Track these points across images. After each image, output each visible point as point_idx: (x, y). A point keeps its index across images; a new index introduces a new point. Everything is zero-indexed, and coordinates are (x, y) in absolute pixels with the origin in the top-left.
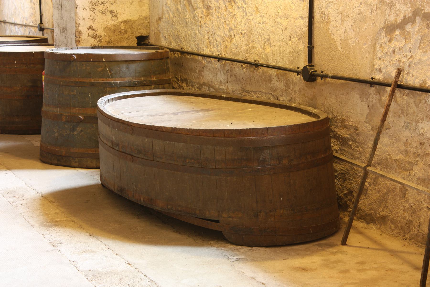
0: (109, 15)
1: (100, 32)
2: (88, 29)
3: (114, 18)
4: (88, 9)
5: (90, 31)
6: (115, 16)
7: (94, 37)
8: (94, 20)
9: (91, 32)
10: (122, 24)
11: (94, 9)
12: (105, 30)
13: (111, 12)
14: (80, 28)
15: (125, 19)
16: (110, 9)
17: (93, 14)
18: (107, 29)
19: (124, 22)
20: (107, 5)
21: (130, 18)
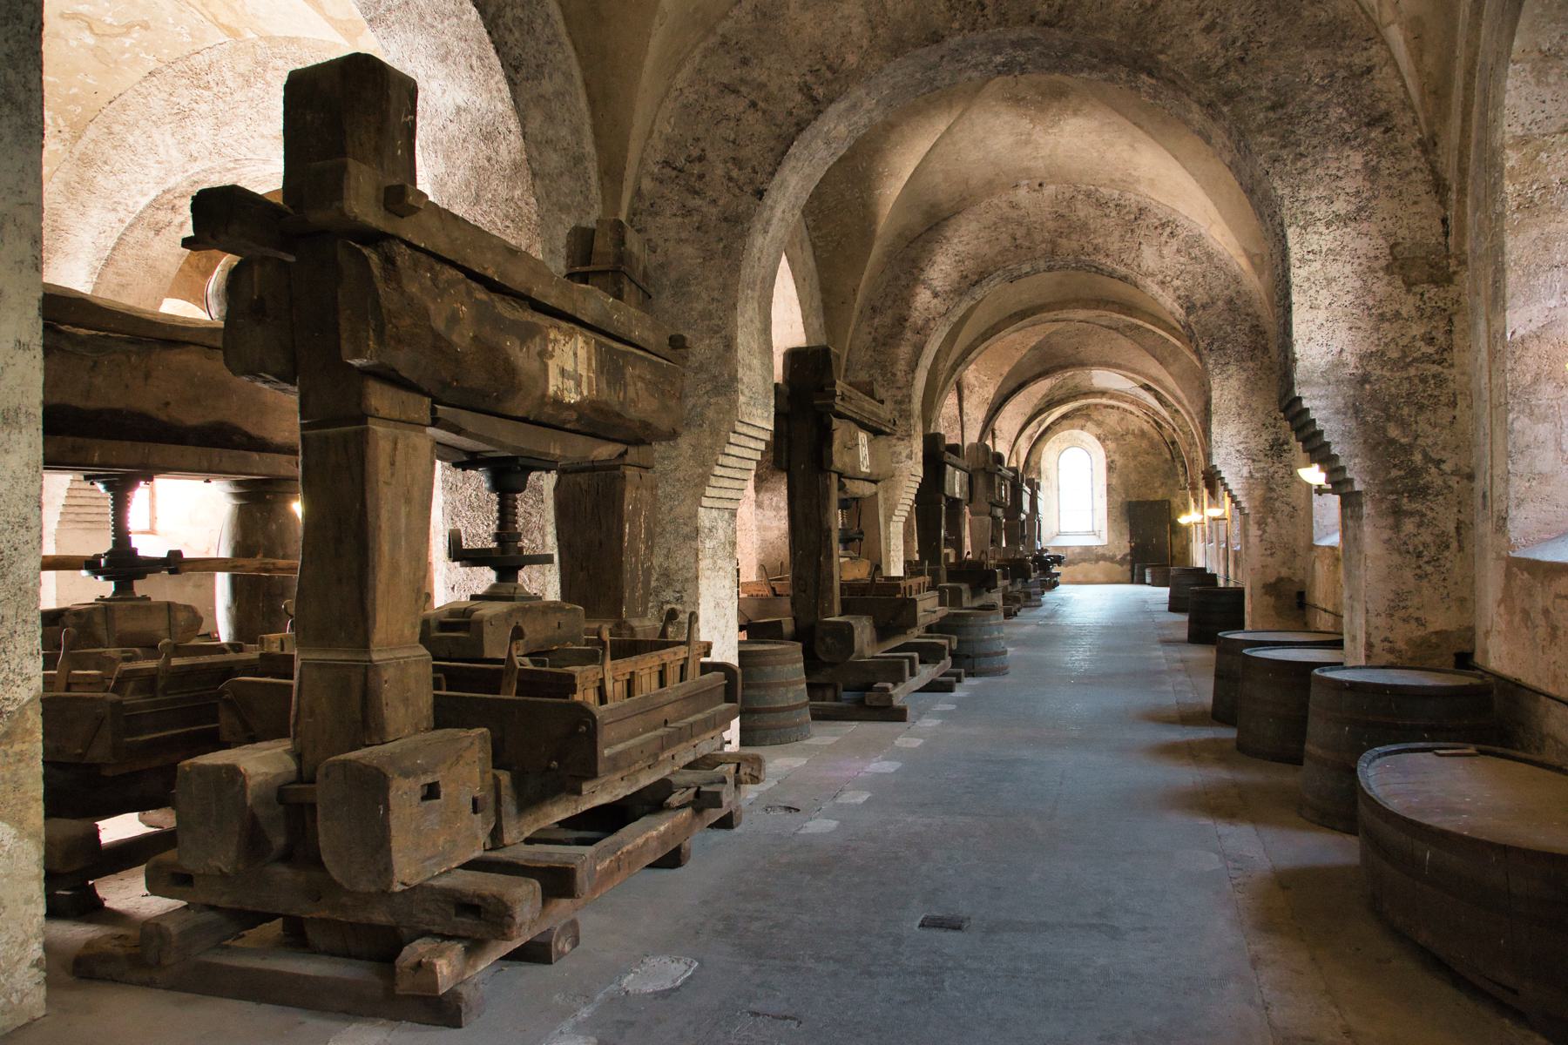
0: (1414, 624)
1: (1401, 645)
2: (1382, 641)
3: (1423, 628)
4: (1383, 615)
5: (1386, 643)
6: (1423, 625)
7: (1391, 651)
8: (1391, 629)
9: (1387, 645)
10: (1434, 636)
11: (1391, 616)
12: (1407, 644)
13: (1417, 619)
14: (1372, 640)
15: (1438, 629)
16: (1415, 615)
17: (1391, 622)
18: (1409, 642)
19: (1436, 633)
20: (1411, 610)
21: (1444, 628)
